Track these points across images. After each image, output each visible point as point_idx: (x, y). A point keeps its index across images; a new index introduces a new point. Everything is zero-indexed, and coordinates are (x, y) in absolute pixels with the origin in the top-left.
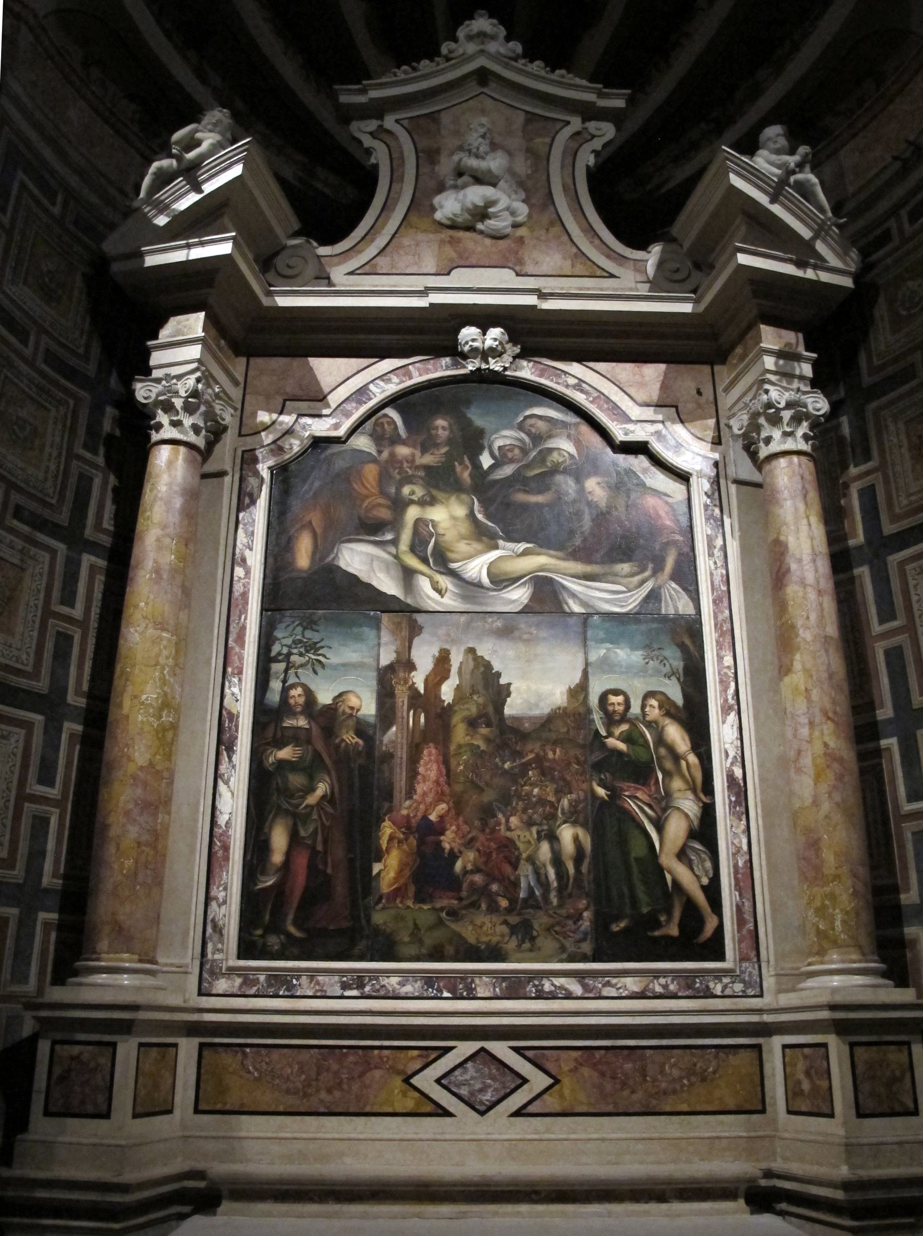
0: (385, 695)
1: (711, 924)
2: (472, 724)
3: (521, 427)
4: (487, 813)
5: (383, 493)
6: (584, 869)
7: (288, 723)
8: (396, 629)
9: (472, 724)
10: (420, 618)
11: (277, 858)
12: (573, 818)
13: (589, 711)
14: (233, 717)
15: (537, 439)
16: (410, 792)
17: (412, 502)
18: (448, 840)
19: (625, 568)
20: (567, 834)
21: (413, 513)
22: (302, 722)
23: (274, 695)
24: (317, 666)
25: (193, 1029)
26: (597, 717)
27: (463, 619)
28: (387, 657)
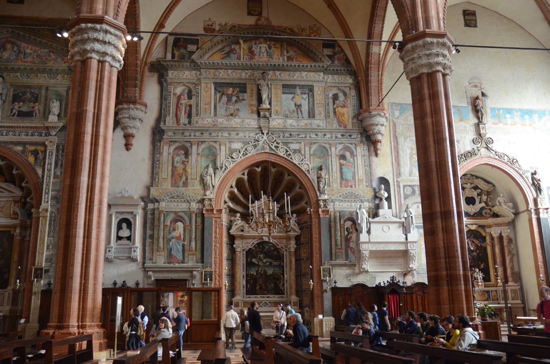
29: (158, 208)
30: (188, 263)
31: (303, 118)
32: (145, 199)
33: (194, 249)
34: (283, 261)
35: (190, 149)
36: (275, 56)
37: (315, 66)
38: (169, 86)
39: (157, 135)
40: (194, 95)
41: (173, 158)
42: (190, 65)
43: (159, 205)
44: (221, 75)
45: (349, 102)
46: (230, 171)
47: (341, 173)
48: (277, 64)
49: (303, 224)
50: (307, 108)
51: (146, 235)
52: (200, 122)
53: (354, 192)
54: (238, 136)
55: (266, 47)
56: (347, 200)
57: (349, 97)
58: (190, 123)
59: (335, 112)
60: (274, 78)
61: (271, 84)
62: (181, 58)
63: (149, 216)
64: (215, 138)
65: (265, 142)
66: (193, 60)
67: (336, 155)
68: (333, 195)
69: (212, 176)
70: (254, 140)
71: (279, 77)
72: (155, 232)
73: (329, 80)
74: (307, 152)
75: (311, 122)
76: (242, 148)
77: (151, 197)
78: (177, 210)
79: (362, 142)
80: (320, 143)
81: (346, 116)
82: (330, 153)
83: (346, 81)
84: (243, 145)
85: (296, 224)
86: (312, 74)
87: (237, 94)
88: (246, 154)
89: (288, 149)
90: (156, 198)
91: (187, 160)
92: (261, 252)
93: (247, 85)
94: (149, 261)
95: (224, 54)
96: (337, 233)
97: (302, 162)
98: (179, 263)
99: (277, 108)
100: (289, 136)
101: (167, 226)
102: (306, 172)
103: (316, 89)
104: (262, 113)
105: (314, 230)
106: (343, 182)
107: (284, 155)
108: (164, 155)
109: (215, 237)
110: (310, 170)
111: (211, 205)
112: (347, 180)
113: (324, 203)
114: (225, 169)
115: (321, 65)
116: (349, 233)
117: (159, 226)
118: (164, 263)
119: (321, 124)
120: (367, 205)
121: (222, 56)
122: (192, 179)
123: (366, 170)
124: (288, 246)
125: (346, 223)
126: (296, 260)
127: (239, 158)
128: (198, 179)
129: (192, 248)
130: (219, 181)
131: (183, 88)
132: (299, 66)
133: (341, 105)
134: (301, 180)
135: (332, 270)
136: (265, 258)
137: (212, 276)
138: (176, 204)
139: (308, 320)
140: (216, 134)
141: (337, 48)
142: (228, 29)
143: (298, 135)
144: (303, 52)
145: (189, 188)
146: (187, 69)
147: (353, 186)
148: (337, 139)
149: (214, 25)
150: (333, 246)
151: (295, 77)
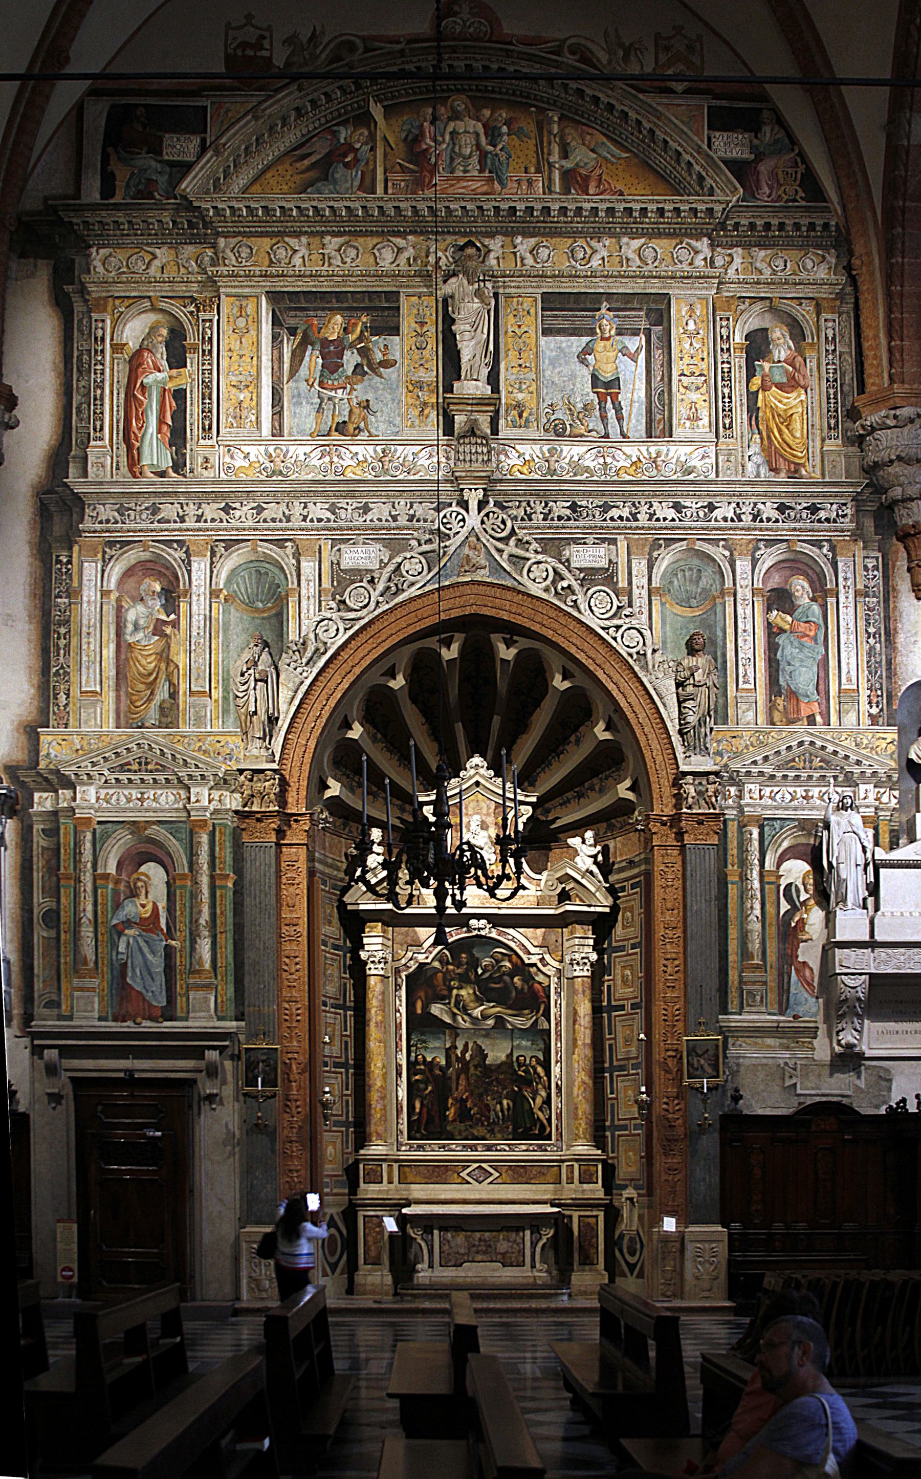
0: (448, 1058)
2: (476, 1067)
3: (492, 957)
4: (481, 1095)
9: (476, 1067)
11: (417, 1110)
14: (401, 1066)
15: (498, 961)
18: (469, 1104)
19: (527, 1012)
20: (505, 1102)
21: (455, 992)
23: (413, 1059)
24: (426, 1048)
25: (396, 1161)
29: (73, 810)
30: (186, 1019)
31: (624, 435)
32: (20, 773)
33: (207, 966)
36: (513, 173)
37: (677, 210)
38: (95, 316)
39: (56, 519)
40: (195, 349)
41: (119, 609)
42: (174, 222)
43: (74, 799)
44: (297, 261)
45: (812, 364)
47: (773, 665)
48: (520, 206)
50: (643, 394)
51: (31, 911)
52: (219, 456)
53: (819, 743)
54: (369, 517)
55: (477, 134)
56: (792, 774)
57: (812, 345)
58: (179, 466)
59: (753, 409)
60: (508, 266)
61: (496, 295)
62: (140, 194)
63: (39, 841)
64: (278, 525)
66: (185, 198)
68: (737, 755)
71: (530, 261)
72: (63, 900)
73: (731, 272)
74: (641, 581)
75: (658, 454)
76: (383, 565)
77: (42, 765)
78: (140, 817)
79: (857, 535)
81: (797, 425)
82: (728, 583)
83: (804, 276)
86: (662, 246)
87: (360, 339)
88: (399, 591)
90: (64, 771)
91: (173, 616)
93: (402, 298)
94: (46, 1012)
95: (308, 169)
97: (616, 622)
98: (151, 1019)
99: (520, 396)
100: (568, 512)
101: (106, 876)
103: (678, 311)
104: (459, 419)
106: (780, 701)
107: (546, 590)
108: (85, 599)
110: (649, 652)
112: (793, 695)
115: (701, 207)
116: (794, 909)
117: (78, 880)
118: (100, 1019)
119: (695, 462)
120: (872, 797)
121: (298, 178)
123: (871, 652)
125: (786, 865)
128: (217, 694)
129: (200, 962)
131: (152, 318)
132: (611, 211)
133: (779, 378)
134: (615, 693)
138: (135, 794)
140: (283, 507)
141: (767, 129)
142: (323, 56)
143: (606, 508)
144: (627, 150)
145: (184, 729)
146: (164, 238)
147: (818, 719)
148: (758, 524)
149: (266, 44)
151: (595, 262)
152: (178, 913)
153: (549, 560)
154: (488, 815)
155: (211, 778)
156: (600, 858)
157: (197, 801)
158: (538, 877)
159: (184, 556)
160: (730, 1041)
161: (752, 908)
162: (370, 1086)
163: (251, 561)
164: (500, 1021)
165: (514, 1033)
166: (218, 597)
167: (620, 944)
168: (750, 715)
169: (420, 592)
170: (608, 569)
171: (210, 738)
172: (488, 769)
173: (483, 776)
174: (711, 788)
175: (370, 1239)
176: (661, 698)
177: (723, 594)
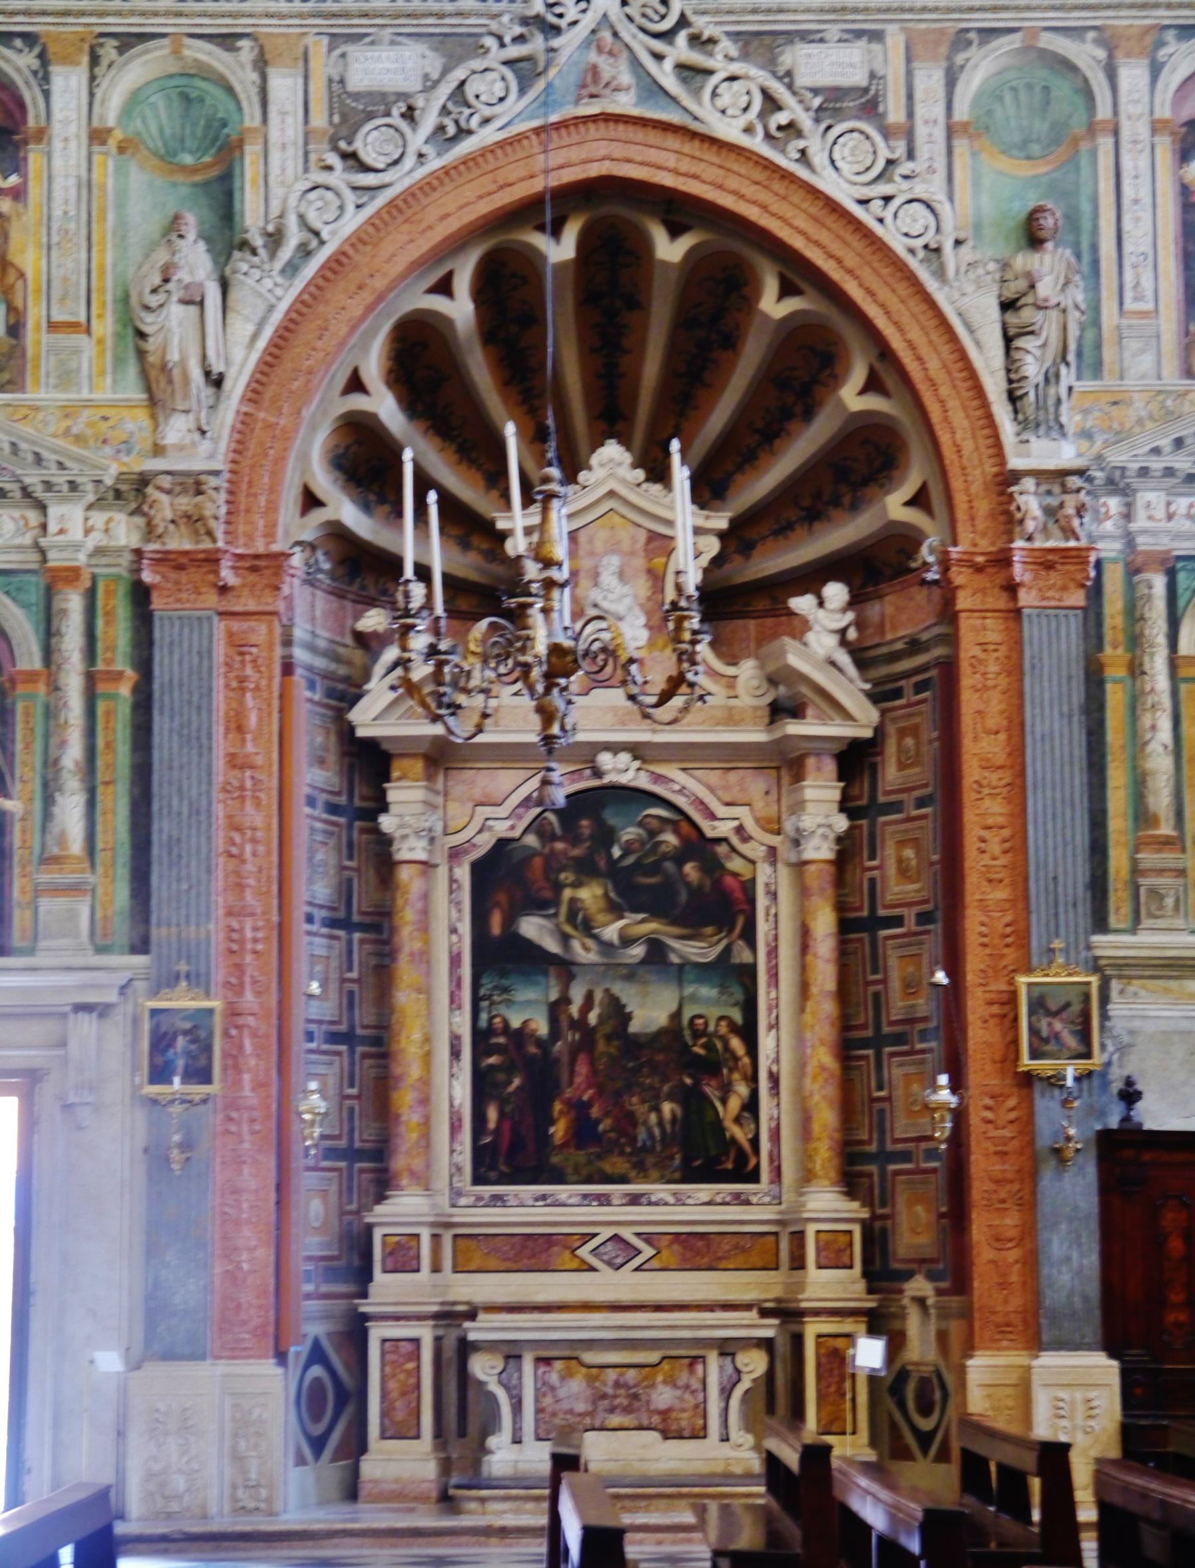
0: (554, 1021)
1: (753, 1162)
2: (609, 1038)
3: (640, 824)
4: (618, 1094)
5: (547, 878)
6: (677, 1128)
7: (494, 1040)
8: (559, 977)
9: (609, 1038)
10: (575, 969)
11: (492, 1124)
12: (671, 1097)
13: (681, 1030)
16: (571, 1083)
17: (566, 886)
18: (595, 1112)
20: (667, 1108)
21: (567, 893)
22: (501, 1040)
24: (509, 1003)
26: (687, 1033)
27: (602, 969)
28: (554, 995)
33: (76, 846)
34: (749, 935)
35: (30, 95)
46: (336, 265)
49: (895, 657)
65: (606, 35)
67: (1157, 127)
68: (1120, 436)
69: (201, 304)
70: (525, 21)
74: (930, 110)
76: (430, 85)
80: (1034, 33)
82: (1103, 111)
84: (433, 64)
85: (844, 659)
88: (463, 132)
89: (779, 90)
91: (13, 180)
92: (586, 870)
96: (1146, 720)
102: (913, 263)
105: (968, 701)
107: (749, 130)
109: (236, 762)
111: (194, 521)
113: (1053, 501)
114: (305, 252)
122: (53, 326)
124: (788, 826)
126: (846, 926)
127: (409, 161)
128: (105, 326)
129: (62, 841)
130: (261, 344)
134: (881, 322)
135: (1105, 999)
136: (616, 910)
137: (208, 1049)
139: (927, 1370)
145: (39, 393)
150: (1118, 822)
152: (19, 747)
153: (753, 71)
154: (632, 553)
155: (90, 487)
156: (852, 634)
157: (61, 532)
158: (731, 671)
159: (35, 64)
160: (1115, 985)
161: (1153, 727)
162: (399, 1079)
163: (171, 76)
164: (657, 951)
165: (682, 972)
166: (103, 143)
167: (893, 798)
168: (1146, 362)
169: (501, 136)
170: (866, 90)
171: (87, 413)
172: (635, 466)
173: (624, 481)
174: (1071, 503)
175: (392, 1385)
176: (971, 331)
177: (1092, 129)
